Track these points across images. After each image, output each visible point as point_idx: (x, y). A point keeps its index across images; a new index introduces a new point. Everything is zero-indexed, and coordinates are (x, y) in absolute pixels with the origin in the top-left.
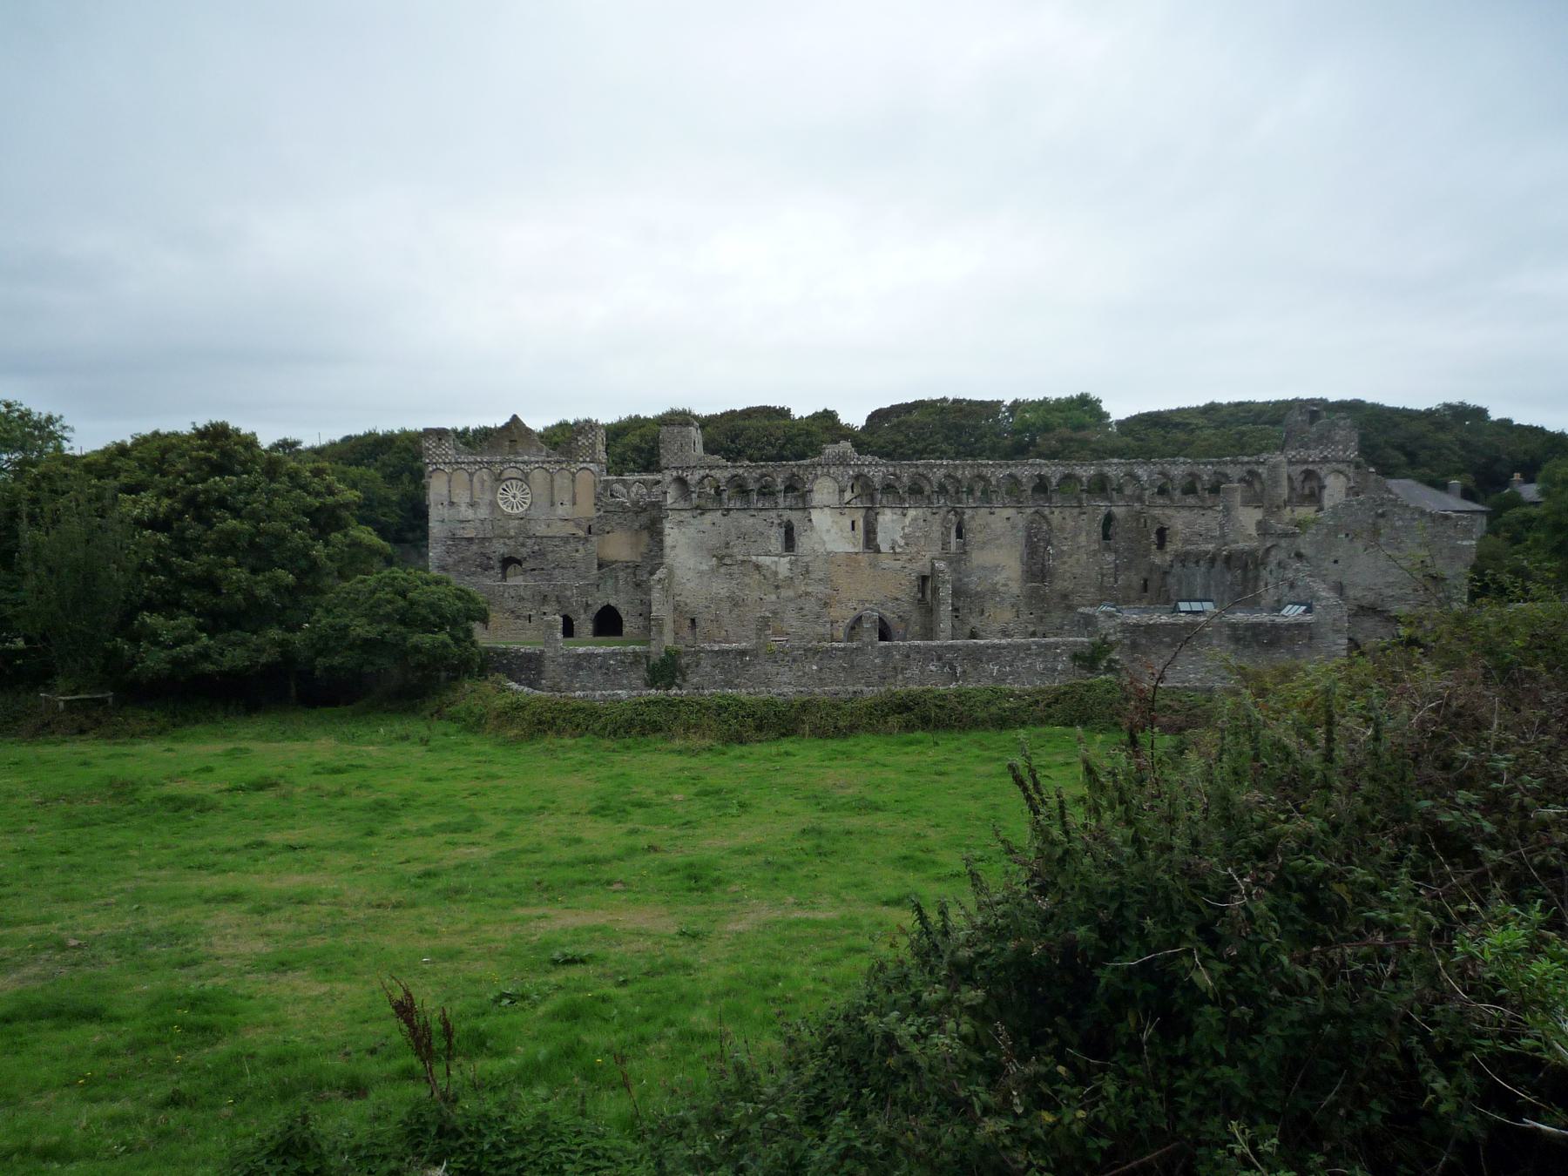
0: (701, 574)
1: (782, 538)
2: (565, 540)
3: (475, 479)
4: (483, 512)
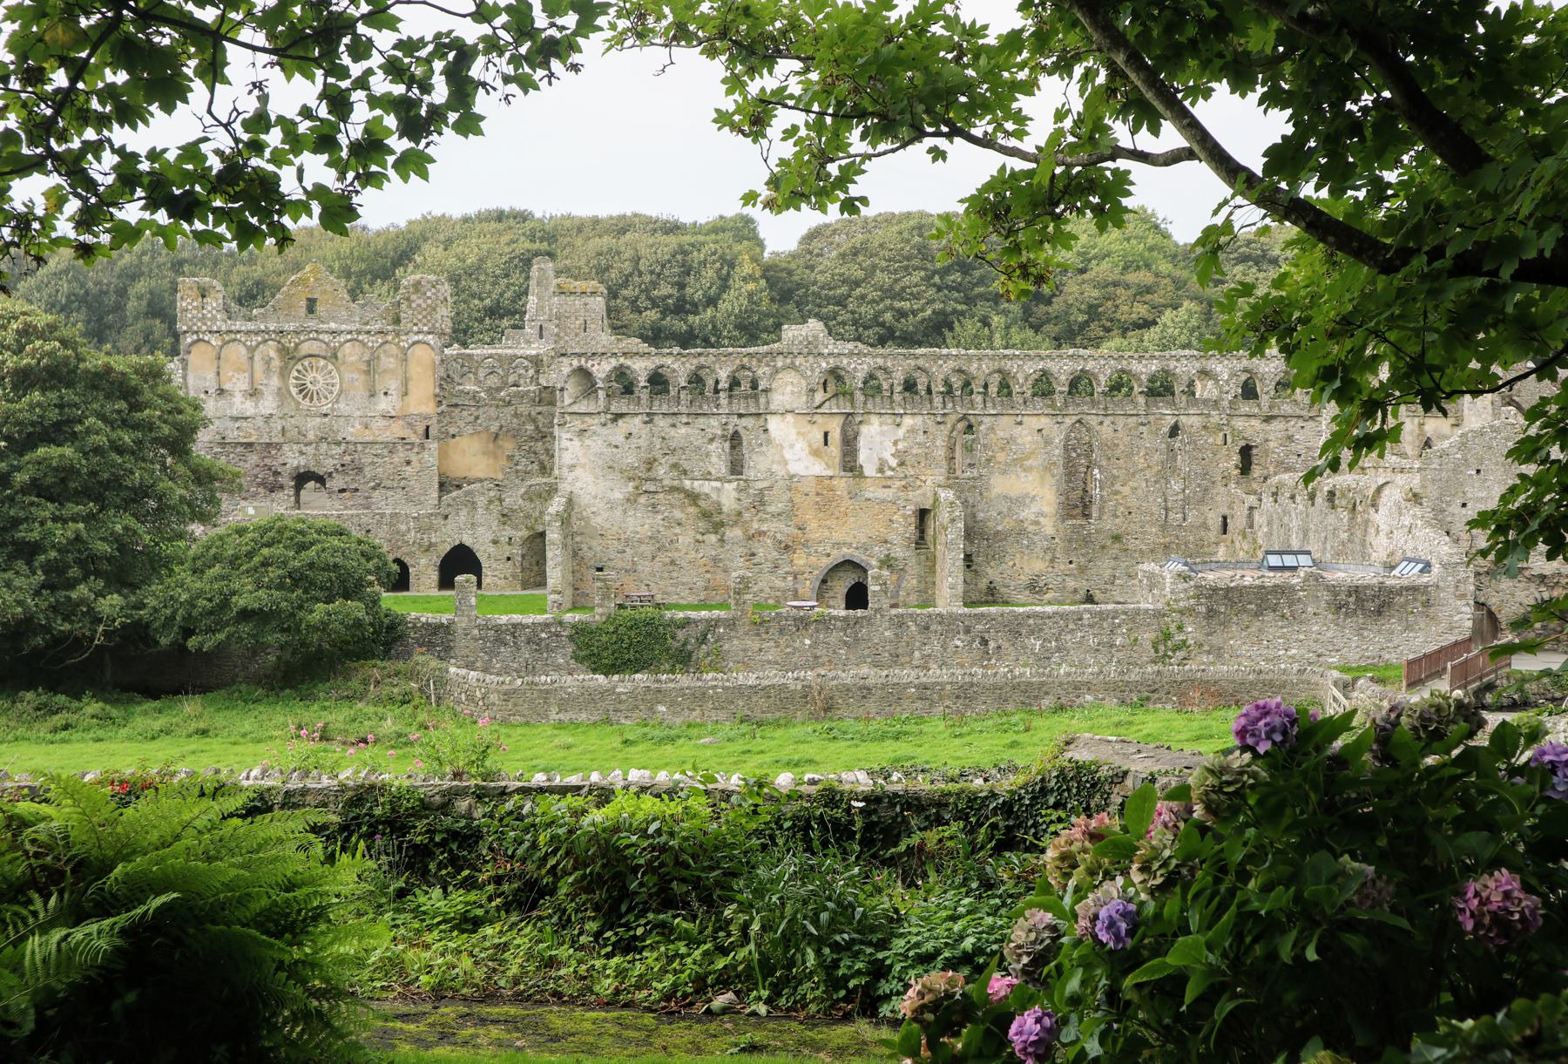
2: (391, 448)
3: (257, 357)
4: (268, 405)
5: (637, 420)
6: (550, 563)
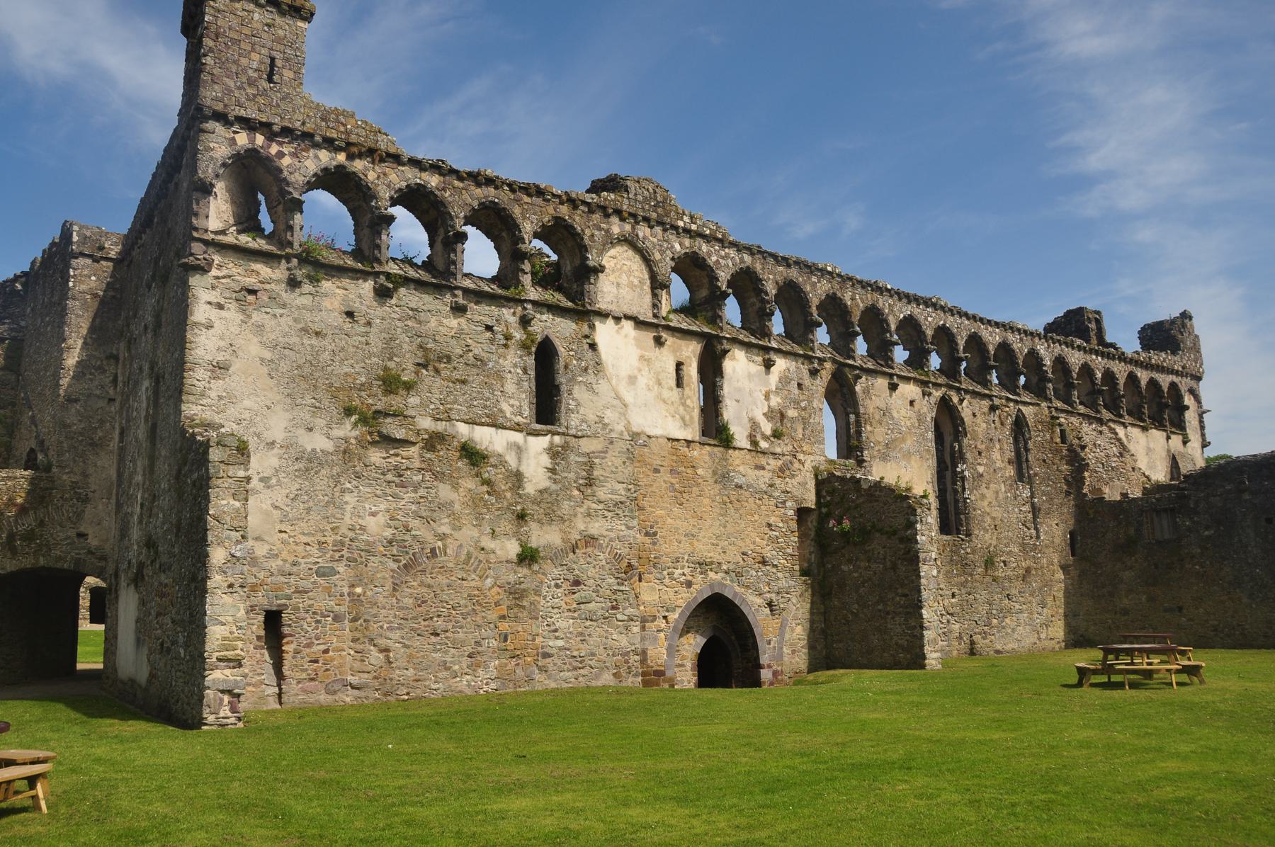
0: (309, 463)
1: (529, 384)
5: (367, 287)
6: (216, 581)
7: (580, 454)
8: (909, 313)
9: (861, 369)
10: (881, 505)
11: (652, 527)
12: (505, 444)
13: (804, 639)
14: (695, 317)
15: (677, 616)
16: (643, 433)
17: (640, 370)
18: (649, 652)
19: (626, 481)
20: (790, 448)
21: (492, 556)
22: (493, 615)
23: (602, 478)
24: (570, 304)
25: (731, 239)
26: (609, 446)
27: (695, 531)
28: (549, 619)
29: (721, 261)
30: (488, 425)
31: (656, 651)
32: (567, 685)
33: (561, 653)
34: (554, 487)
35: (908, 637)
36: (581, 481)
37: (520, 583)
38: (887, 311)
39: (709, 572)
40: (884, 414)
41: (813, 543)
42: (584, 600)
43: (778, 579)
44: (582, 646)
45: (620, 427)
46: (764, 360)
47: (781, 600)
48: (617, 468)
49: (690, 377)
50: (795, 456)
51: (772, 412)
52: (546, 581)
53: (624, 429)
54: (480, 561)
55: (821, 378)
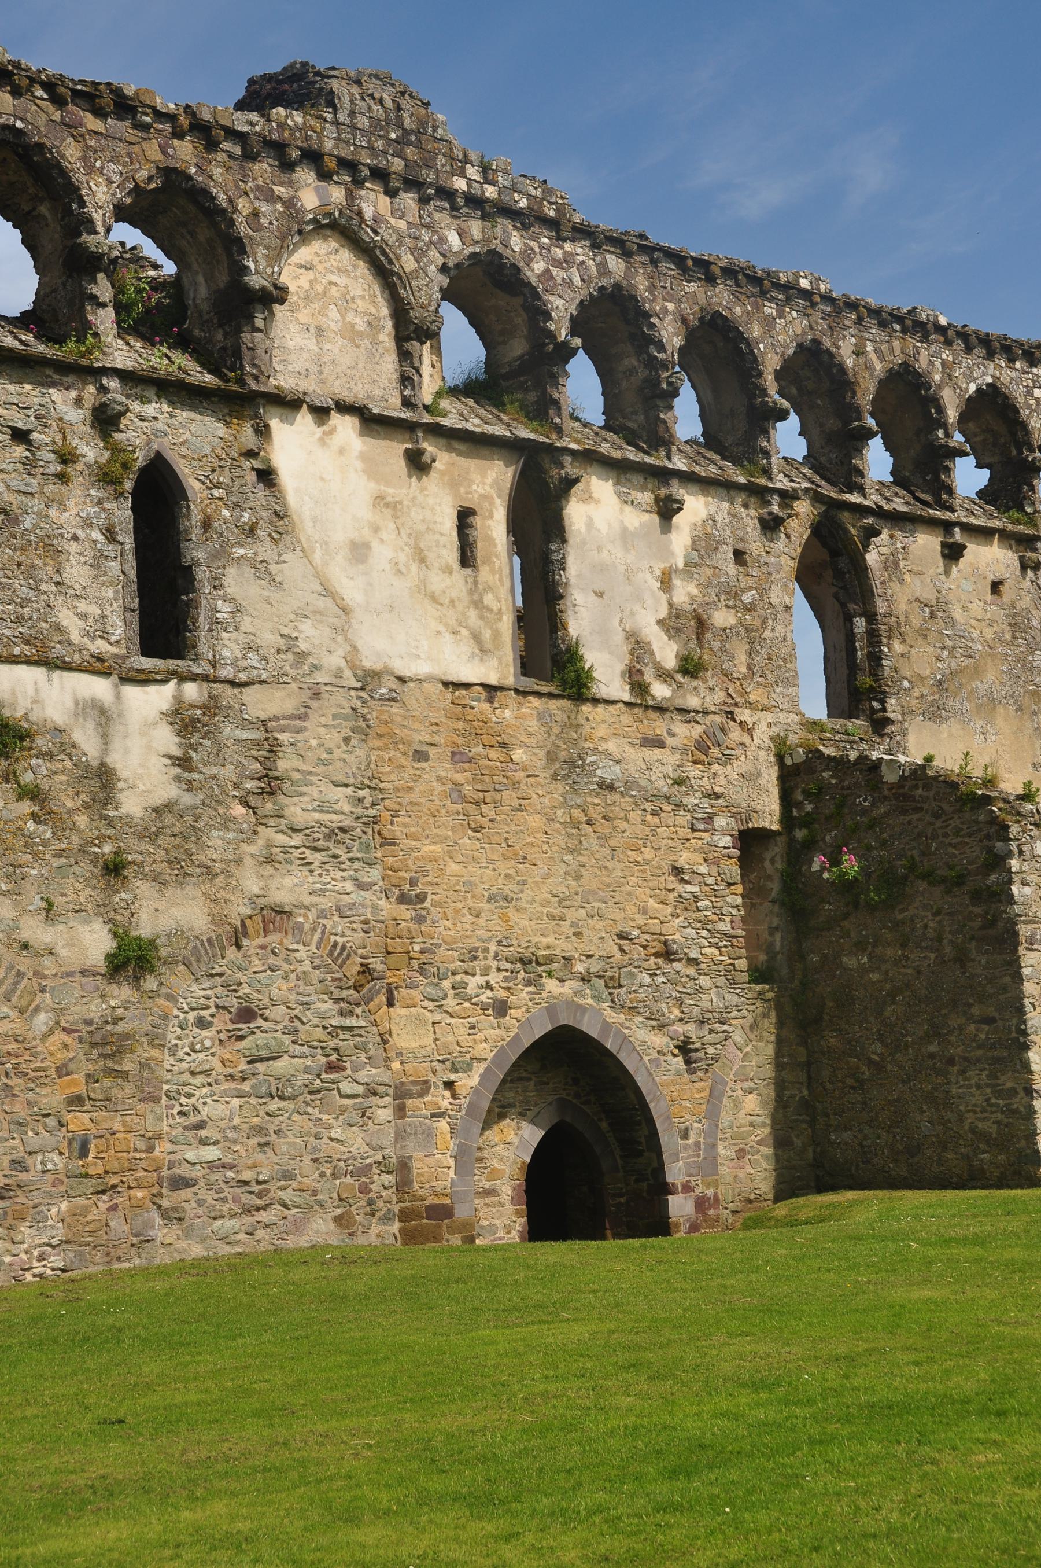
7: (245, 723)
8: (989, 380)
9: (879, 513)
10: (928, 818)
11: (413, 882)
12: (70, 704)
13: (764, 1125)
14: (500, 405)
15: (474, 1080)
16: (387, 671)
17: (376, 529)
18: (414, 1165)
19: (351, 781)
20: (720, 696)
21: (47, 961)
22: (52, 1098)
23: (296, 776)
24: (209, 379)
25: (577, 218)
26: (310, 703)
27: (510, 888)
28: (183, 1100)
29: (554, 271)
30: (28, 662)
31: (430, 1161)
32: (225, 1250)
33: (214, 1177)
34: (188, 799)
35: (1000, 1116)
36: (249, 785)
37: (116, 1020)
38: (937, 378)
39: (545, 980)
40: (933, 616)
41: (776, 908)
42: (264, 1053)
43: (700, 990)
44: (261, 1156)
45: (335, 660)
46: (657, 500)
47: (709, 1038)
48: (330, 752)
49: (490, 540)
50: (730, 715)
51: (677, 616)
52: (176, 1012)
53: (343, 664)
54: (20, 975)
55: (788, 537)
